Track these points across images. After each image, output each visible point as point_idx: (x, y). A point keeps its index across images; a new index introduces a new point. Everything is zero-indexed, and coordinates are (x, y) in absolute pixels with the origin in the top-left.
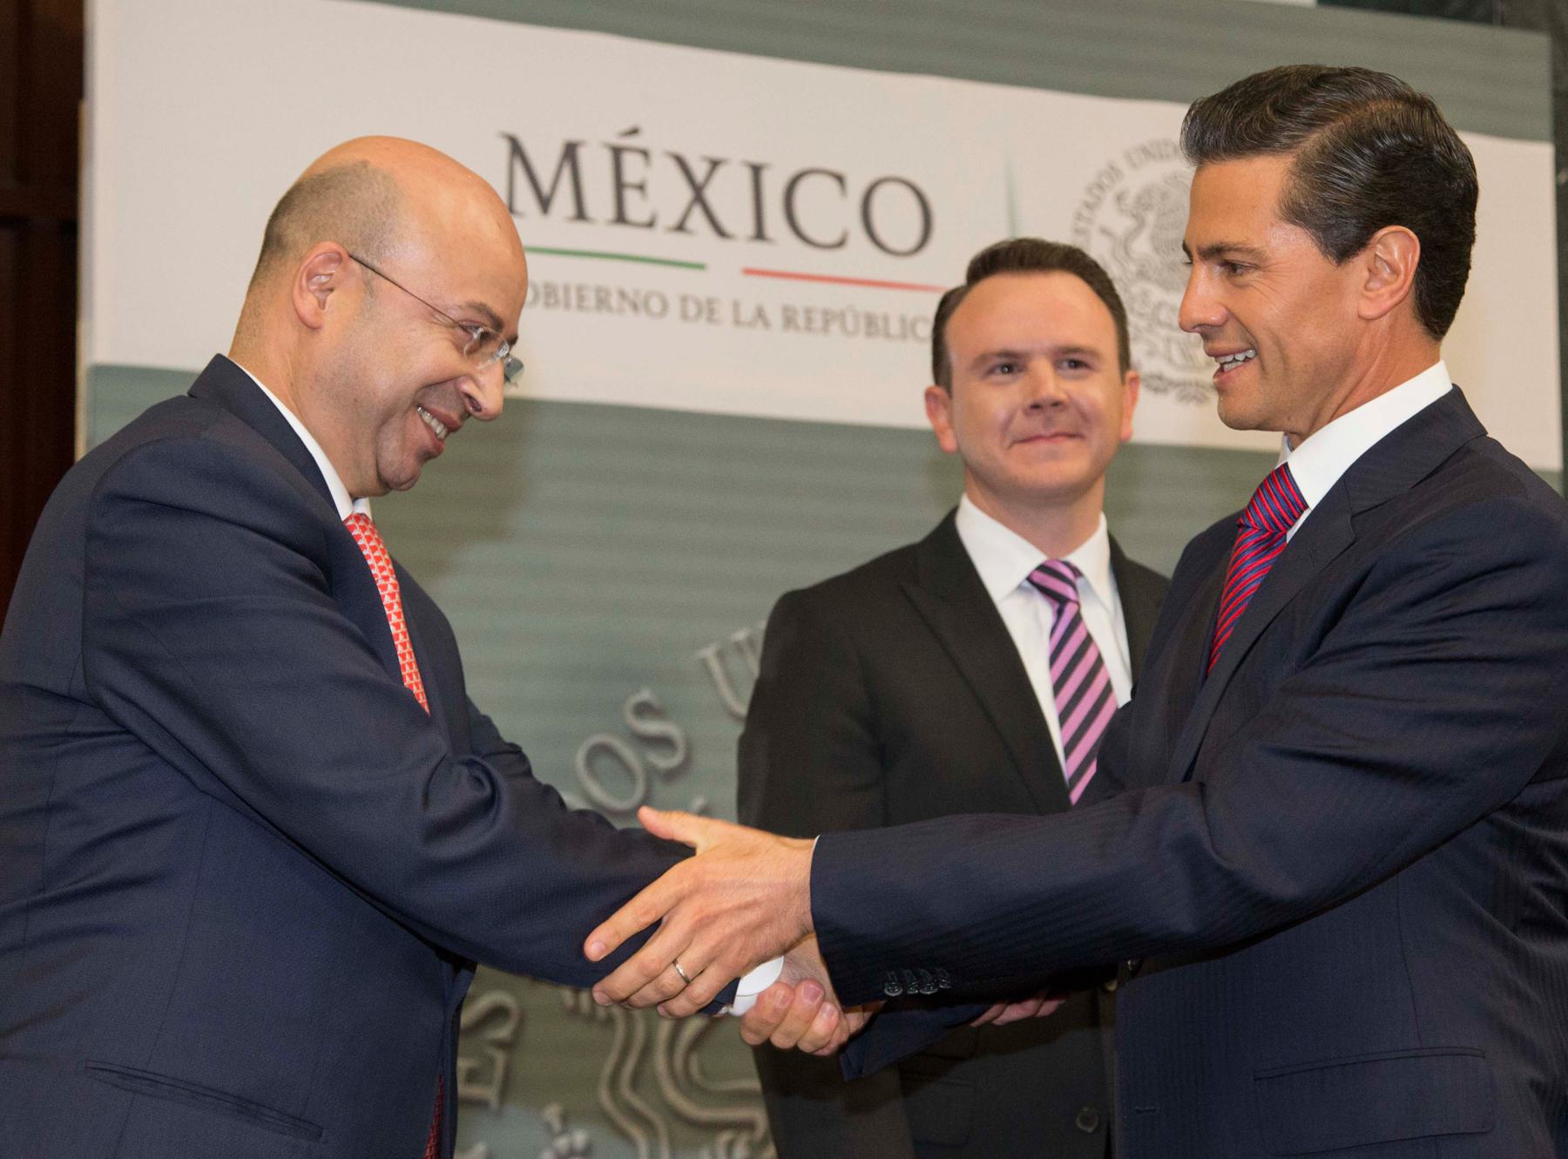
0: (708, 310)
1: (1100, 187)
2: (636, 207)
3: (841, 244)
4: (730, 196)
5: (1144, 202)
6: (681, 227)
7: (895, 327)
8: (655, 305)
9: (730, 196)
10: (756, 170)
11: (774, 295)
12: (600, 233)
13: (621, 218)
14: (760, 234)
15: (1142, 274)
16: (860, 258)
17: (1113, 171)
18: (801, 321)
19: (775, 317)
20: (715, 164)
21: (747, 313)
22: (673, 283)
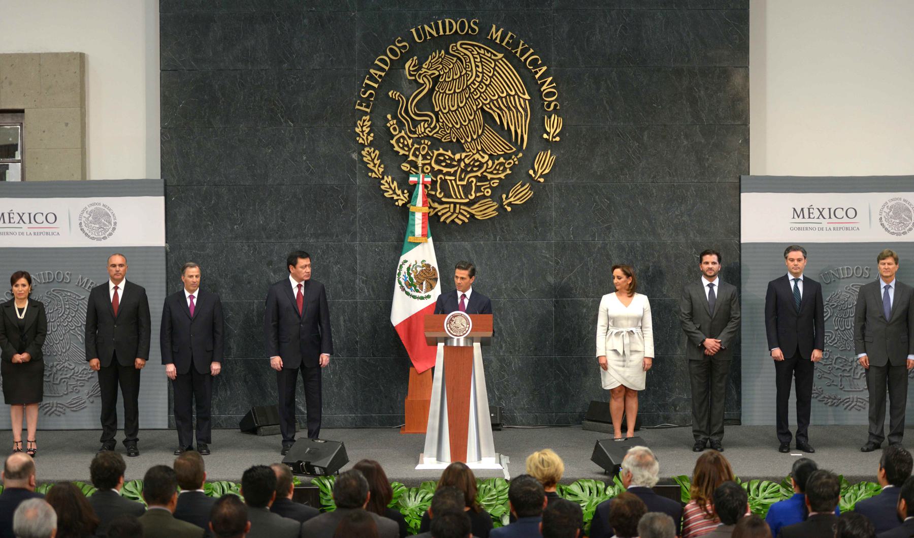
0: (23, 234)
1: (84, 210)
2: (12, 221)
3: (43, 222)
4: (26, 218)
5: (91, 212)
6: (19, 223)
7: (51, 234)
8: (15, 233)
9: (26, 218)
10: (30, 214)
11: (32, 231)
12: (7, 225)
13: (10, 222)
14: (30, 222)
15: (91, 223)
16: (46, 224)
17: (86, 208)
18: (36, 234)
19: (33, 234)
20: (23, 214)
21: (28, 234)
22: (17, 230)
